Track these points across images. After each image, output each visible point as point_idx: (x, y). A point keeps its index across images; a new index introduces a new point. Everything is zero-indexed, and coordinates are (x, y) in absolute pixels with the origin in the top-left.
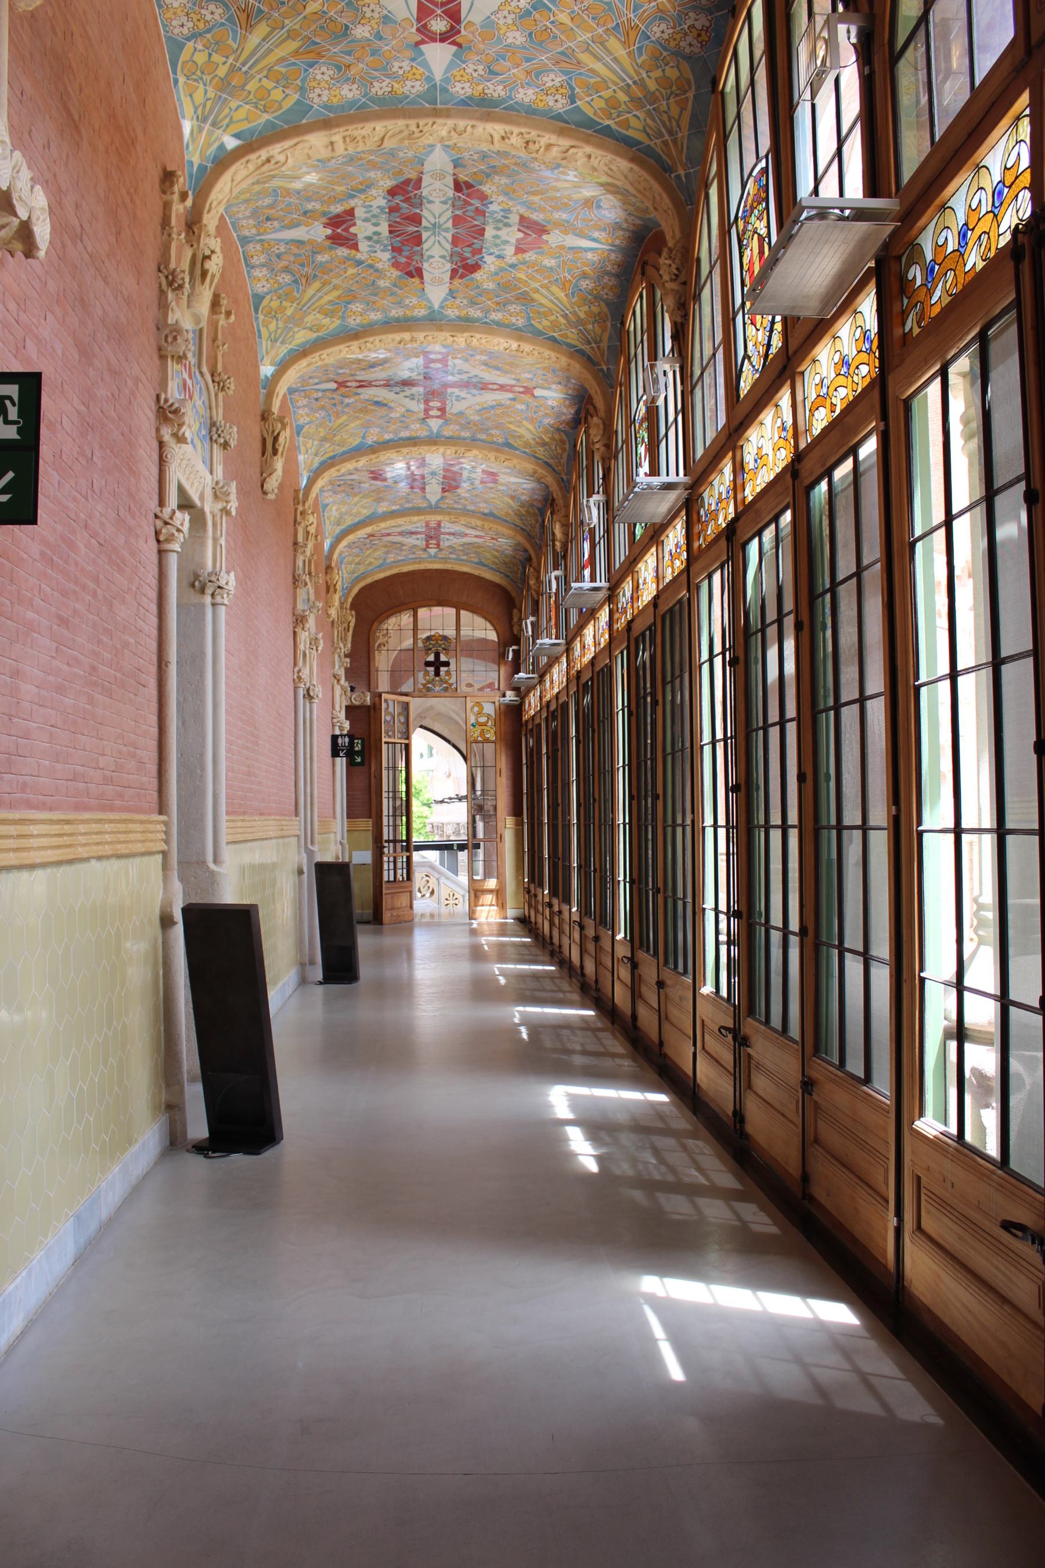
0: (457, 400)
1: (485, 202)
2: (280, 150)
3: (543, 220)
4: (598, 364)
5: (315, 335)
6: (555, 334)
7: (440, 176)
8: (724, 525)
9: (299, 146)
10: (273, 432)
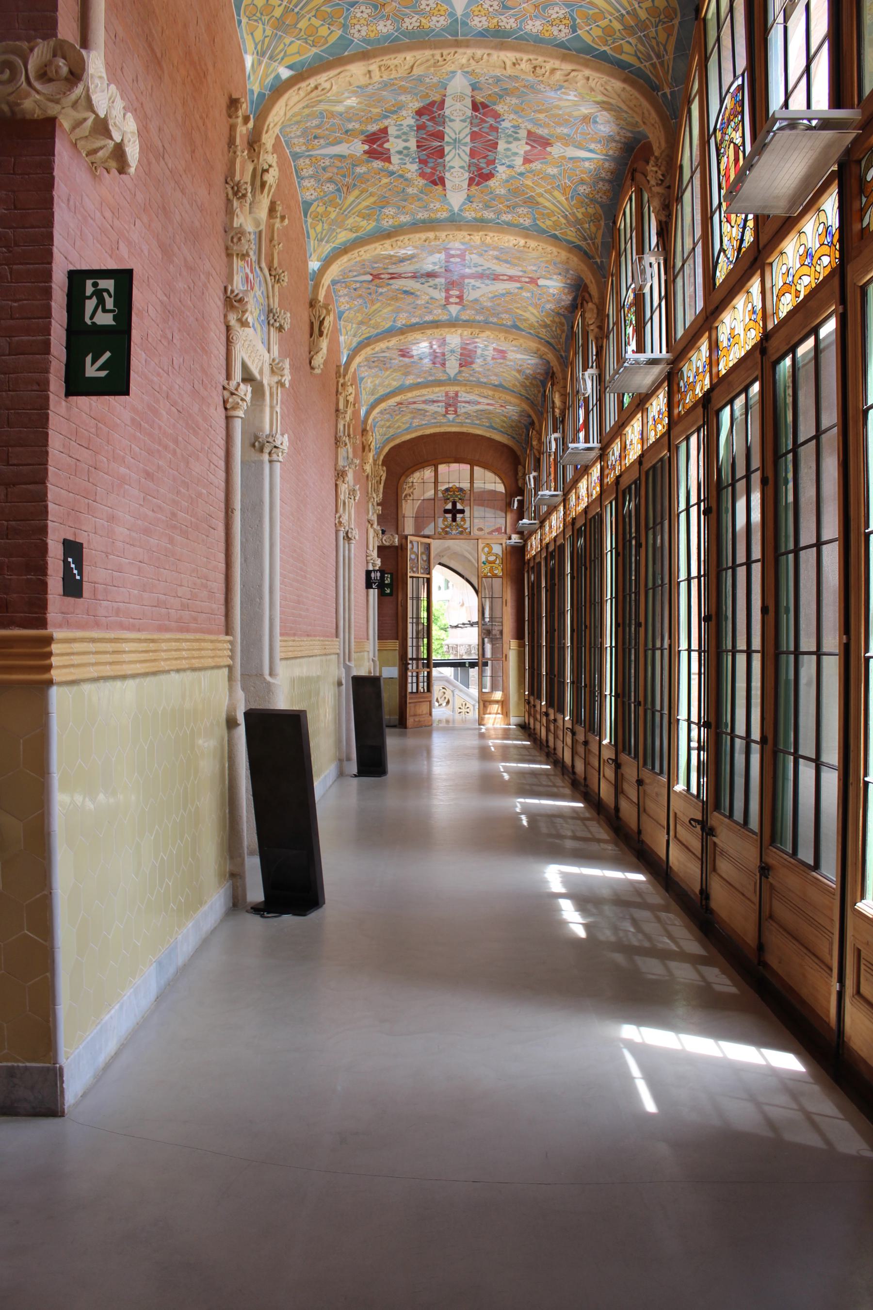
1: (498, 120)
2: (326, 79)
3: (548, 135)
4: (593, 258)
5: (354, 235)
6: (556, 233)
7: (460, 98)
8: (700, 395)
9: (342, 75)
10: (319, 317)
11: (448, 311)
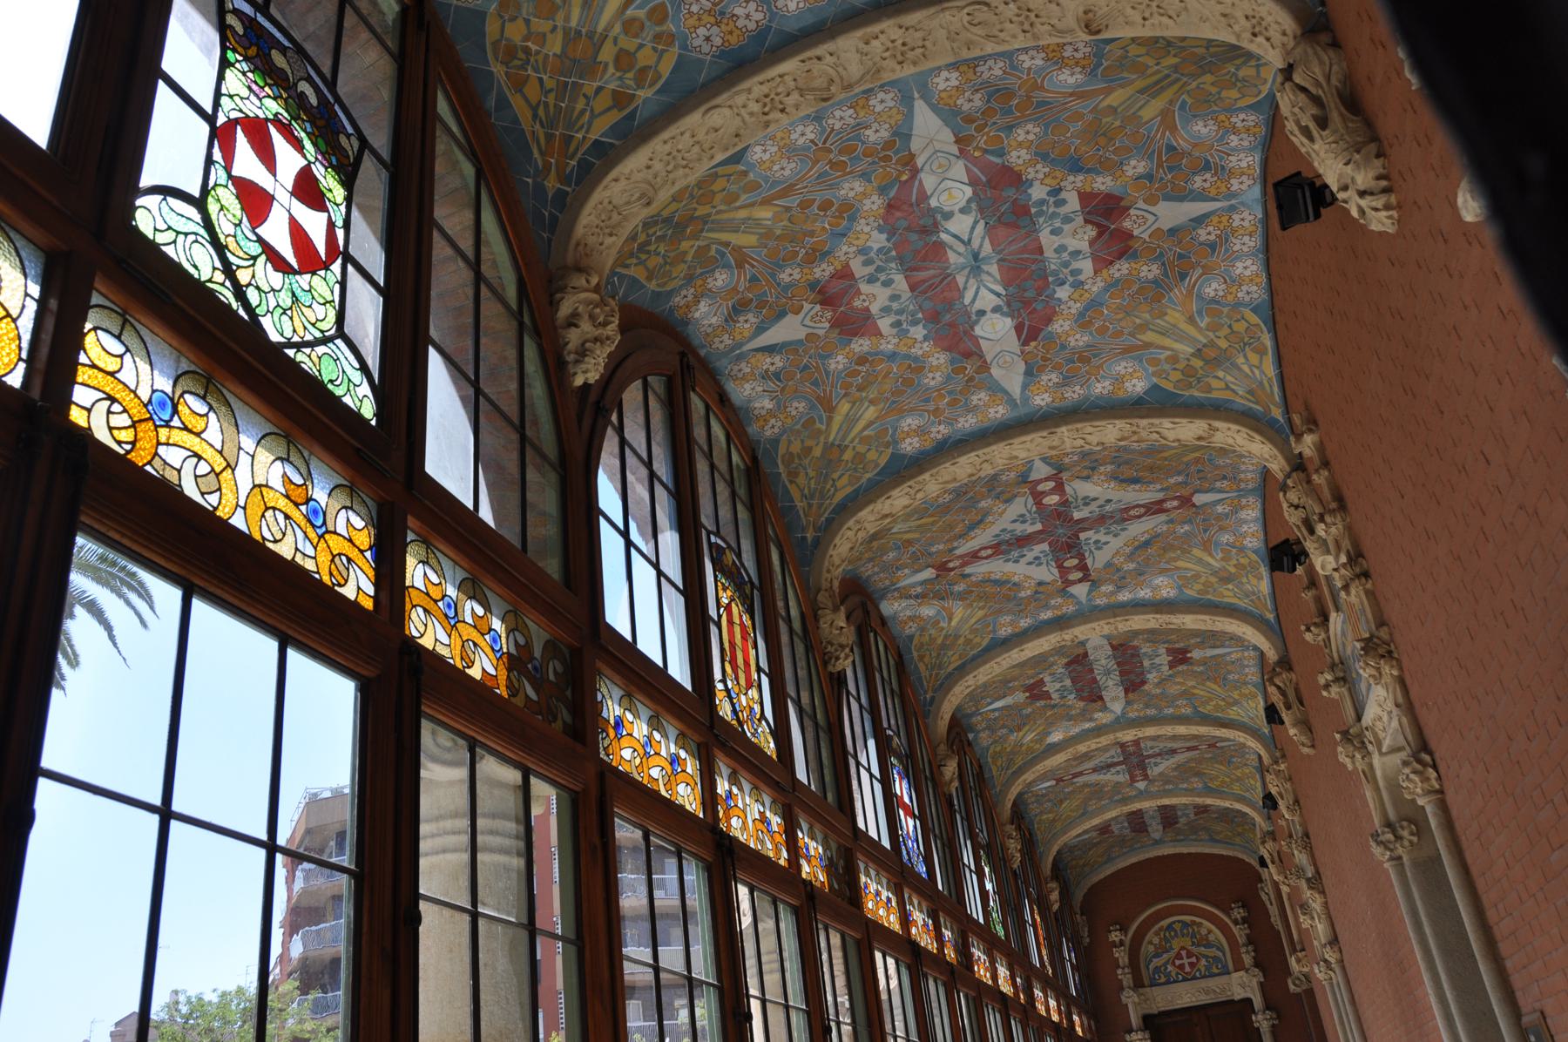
0: (1099, 549)
11: (1072, 596)
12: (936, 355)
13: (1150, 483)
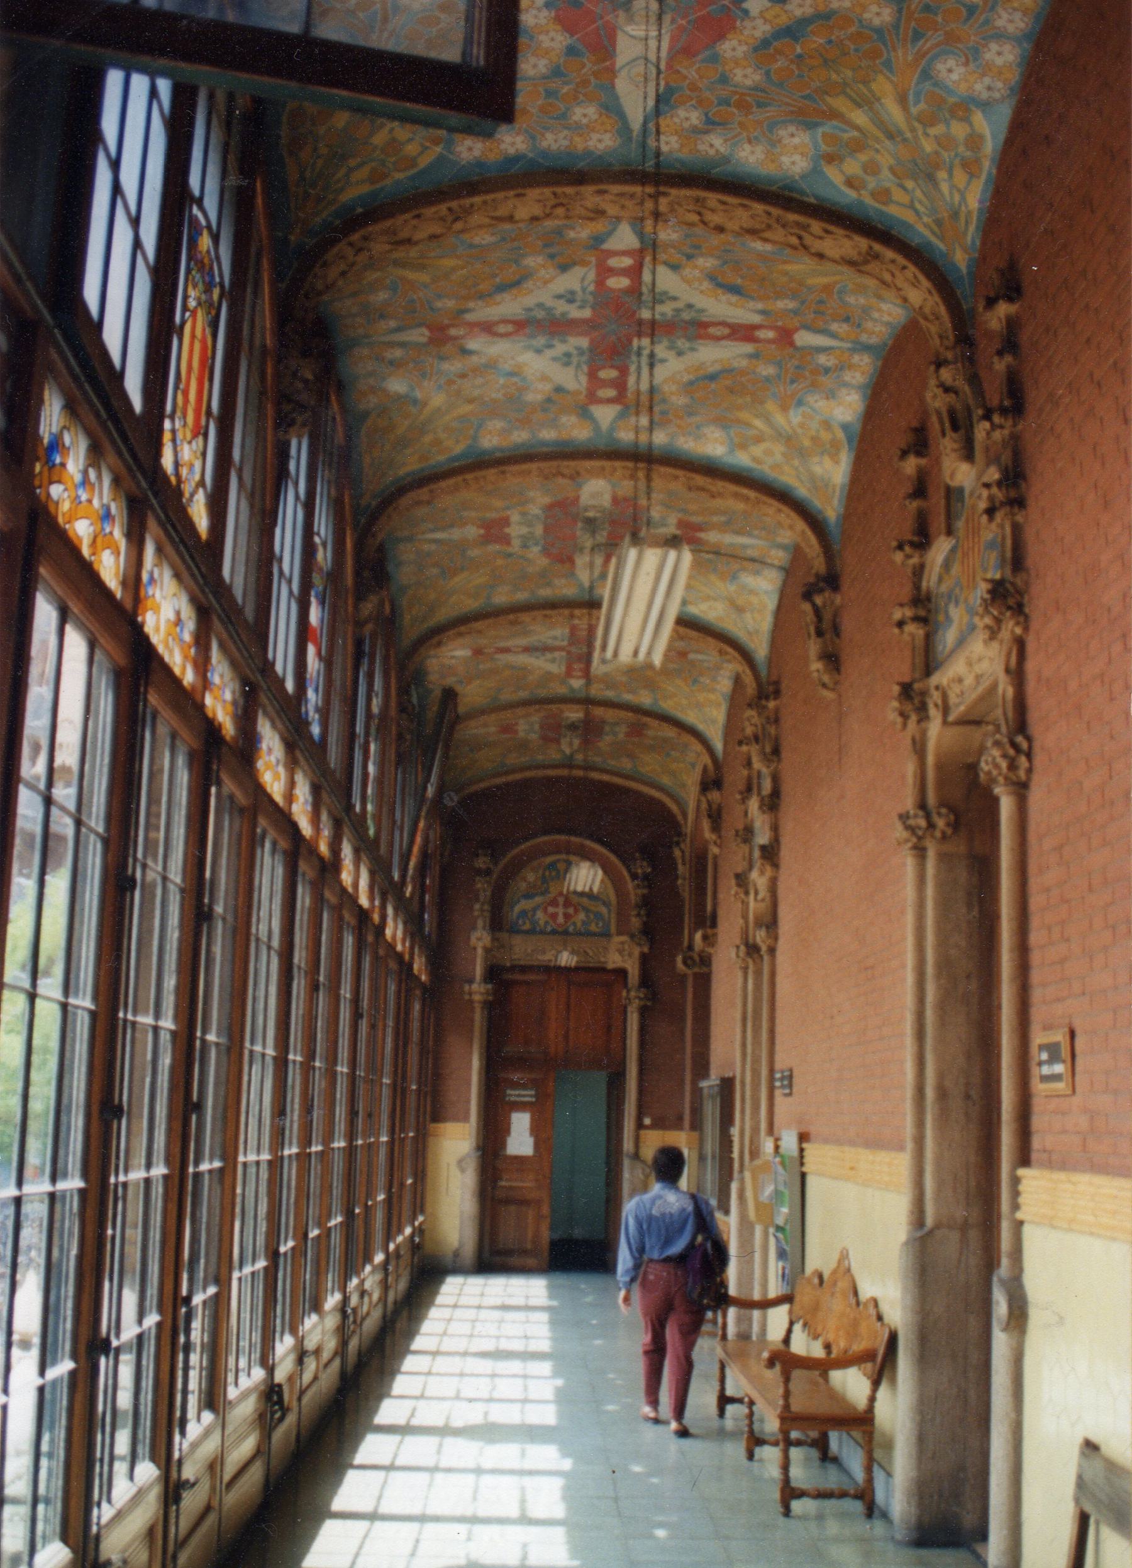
12: (552, 34)
13: (753, 299)
